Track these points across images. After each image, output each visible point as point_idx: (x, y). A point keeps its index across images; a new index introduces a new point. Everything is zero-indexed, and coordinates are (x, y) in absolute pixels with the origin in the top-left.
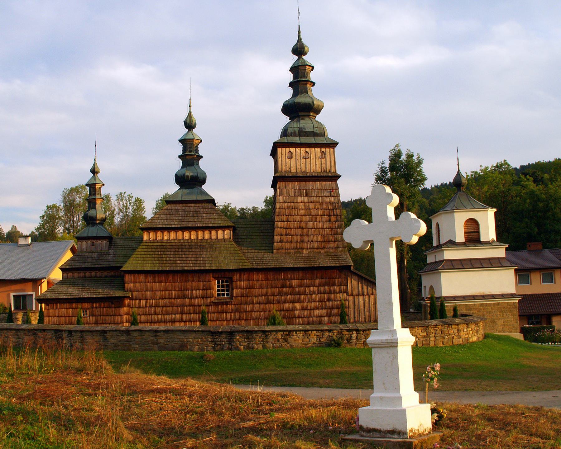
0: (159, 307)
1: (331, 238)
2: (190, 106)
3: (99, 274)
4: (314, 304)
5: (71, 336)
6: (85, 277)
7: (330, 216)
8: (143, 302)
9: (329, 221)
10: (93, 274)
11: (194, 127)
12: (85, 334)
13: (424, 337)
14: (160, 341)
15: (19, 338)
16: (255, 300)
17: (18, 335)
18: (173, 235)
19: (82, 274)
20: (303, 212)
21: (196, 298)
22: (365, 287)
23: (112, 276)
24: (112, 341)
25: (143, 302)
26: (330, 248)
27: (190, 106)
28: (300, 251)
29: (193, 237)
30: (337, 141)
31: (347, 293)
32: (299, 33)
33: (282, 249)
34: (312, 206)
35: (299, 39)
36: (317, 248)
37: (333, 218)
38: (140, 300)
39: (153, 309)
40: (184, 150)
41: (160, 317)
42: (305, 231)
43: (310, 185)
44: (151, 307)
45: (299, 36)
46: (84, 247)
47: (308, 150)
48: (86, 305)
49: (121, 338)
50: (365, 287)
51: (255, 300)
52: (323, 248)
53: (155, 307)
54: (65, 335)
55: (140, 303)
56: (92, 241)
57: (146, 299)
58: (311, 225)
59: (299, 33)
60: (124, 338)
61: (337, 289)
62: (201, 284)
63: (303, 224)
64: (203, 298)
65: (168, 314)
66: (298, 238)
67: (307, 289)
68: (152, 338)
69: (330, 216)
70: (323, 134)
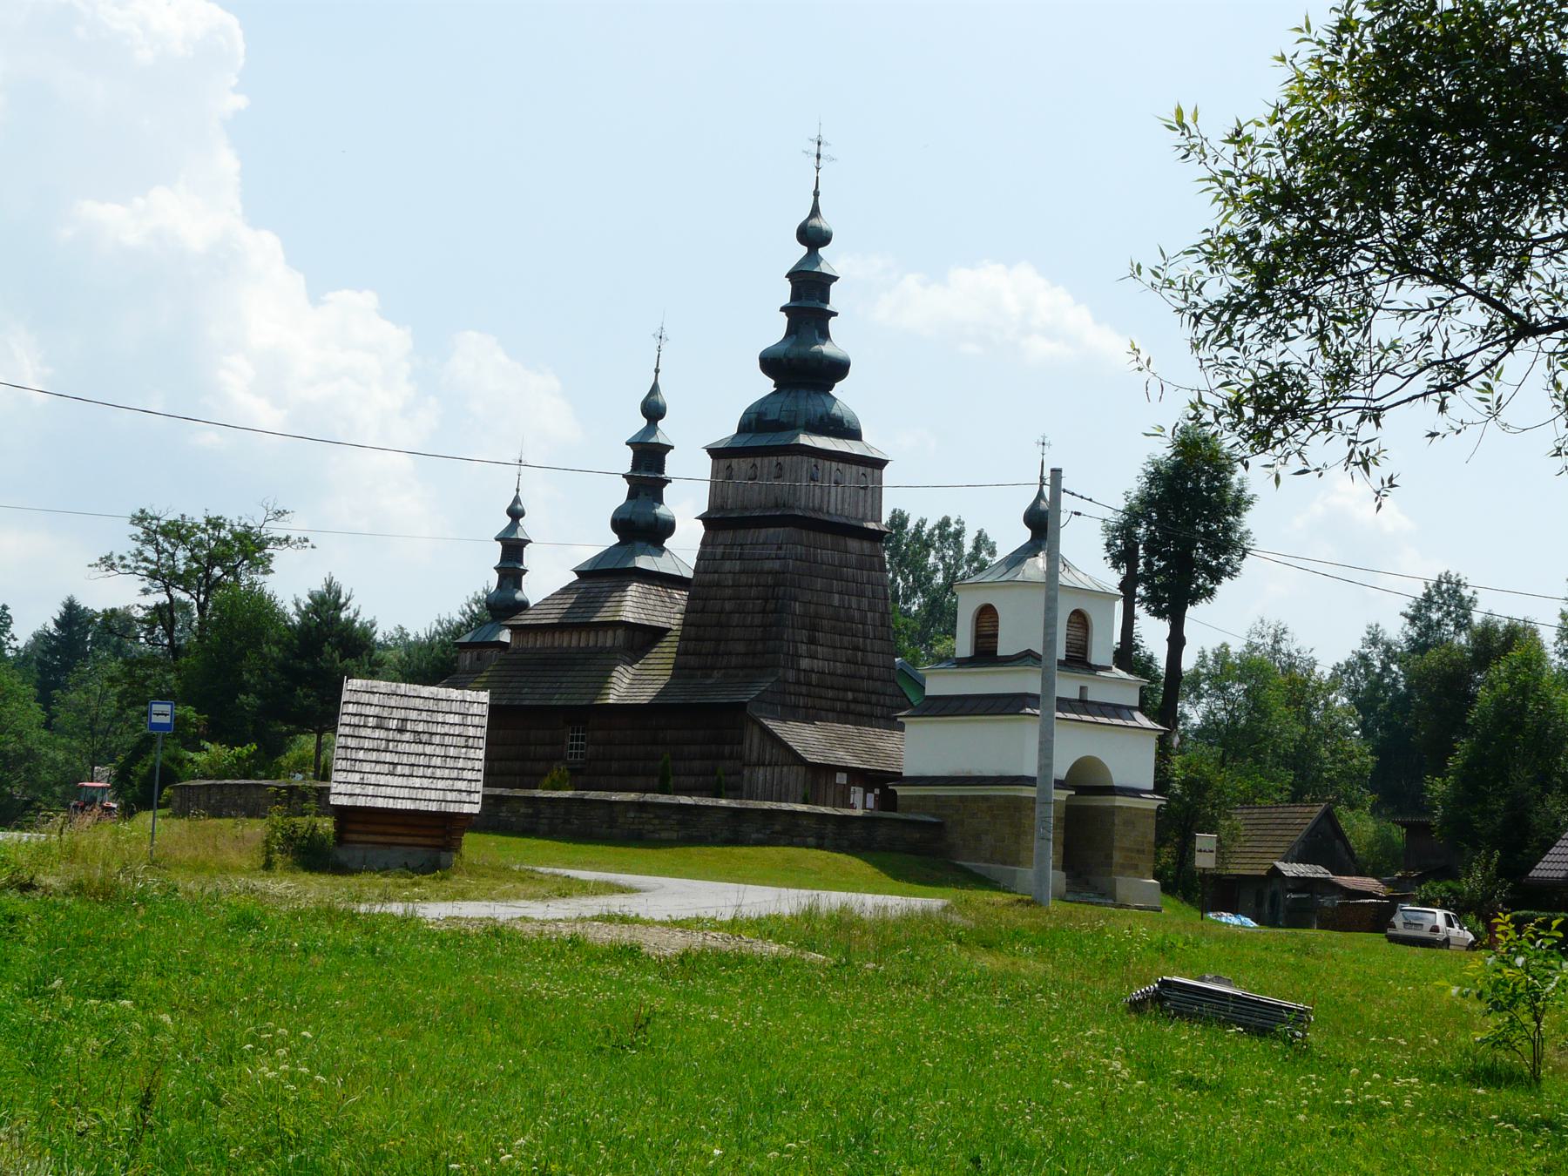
1: (760, 646)
2: (657, 371)
7: (766, 600)
9: (763, 612)
11: (662, 416)
13: (527, 816)
20: (728, 592)
27: (657, 371)
29: (574, 643)
32: (816, 194)
35: (815, 211)
37: (771, 605)
40: (635, 466)
43: (752, 535)
45: (816, 201)
58: (736, 618)
59: (816, 194)
61: (727, 749)
69: (766, 600)
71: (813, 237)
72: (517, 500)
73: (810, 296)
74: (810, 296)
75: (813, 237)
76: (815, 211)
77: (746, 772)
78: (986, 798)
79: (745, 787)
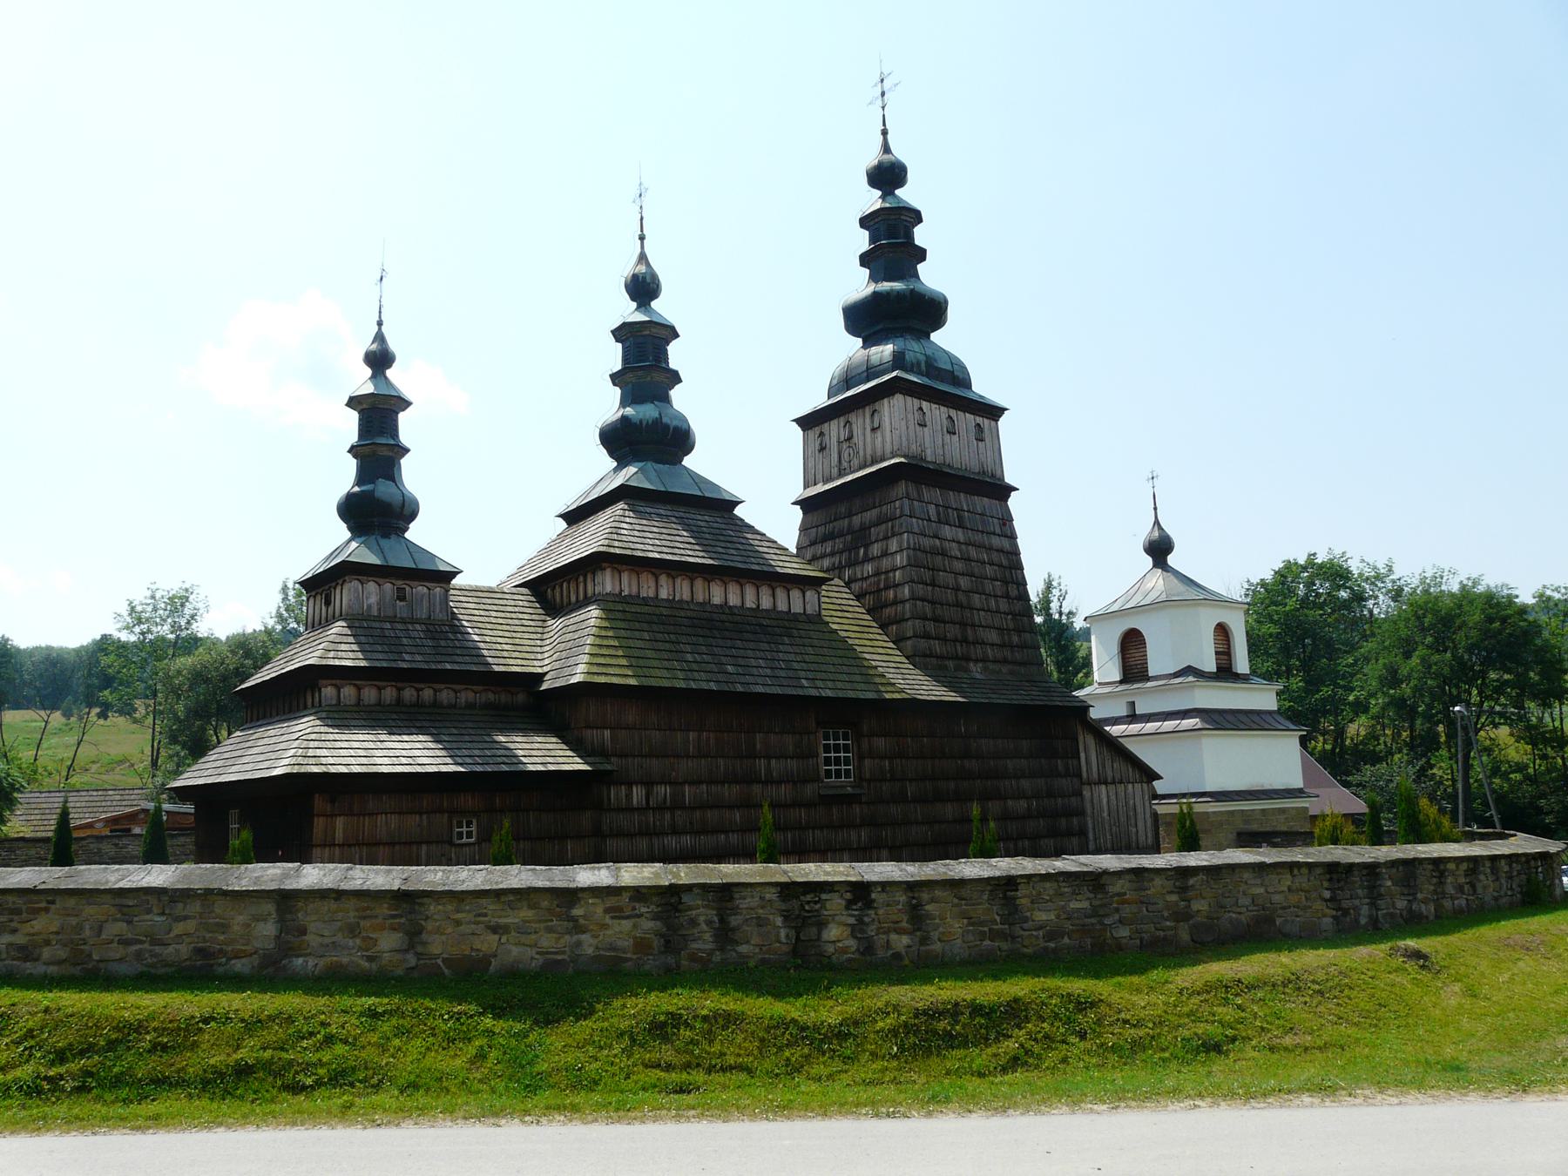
0: (683, 808)
1: (1015, 639)
2: (642, 238)
3: (446, 696)
4: (1023, 804)
5: (869, 904)
6: (399, 701)
8: (638, 794)
9: (1007, 596)
10: (409, 694)
12: (925, 896)
14: (1200, 906)
15: (579, 929)
16: (910, 789)
17: (574, 919)
18: (683, 590)
19: (389, 694)
21: (779, 782)
22: (1108, 764)
23: (488, 706)
24: (1041, 916)
25: (638, 794)
26: (1014, 663)
27: (642, 238)
28: (964, 663)
30: (1001, 402)
31: (1080, 776)
32: (885, 133)
33: (931, 656)
34: (973, 552)
35: (886, 149)
36: (994, 662)
38: (630, 784)
39: (668, 816)
41: (687, 840)
42: (967, 613)
44: (661, 808)
46: (373, 600)
47: (953, 413)
48: (467, 801)
49: (1074, 905)
50: (1108, 764)
51: (910, 789)
52: (1005, 661)
53: (672, 809)
54: (835, 903)
55: (629, 796)
56: (399, 583)
57: (649, 784)
58: (976, 600)
59: (885, 133)
60: (1085, 904)
62: (789, 741)
63: (961, 597)
64: (794, 783)
65: (704, 832)
66: (953, 631)
67: (1010, 764)
68: (1174, 898)
70: (967, 384)
71: (887, 176)
72: (380, 337)
73: (892, 238)
74: (892, 238)
75: (887, 176)
76: (886, 149)
77: (1086, 793)
78: (1283, 811)
79: (1089, 811)
